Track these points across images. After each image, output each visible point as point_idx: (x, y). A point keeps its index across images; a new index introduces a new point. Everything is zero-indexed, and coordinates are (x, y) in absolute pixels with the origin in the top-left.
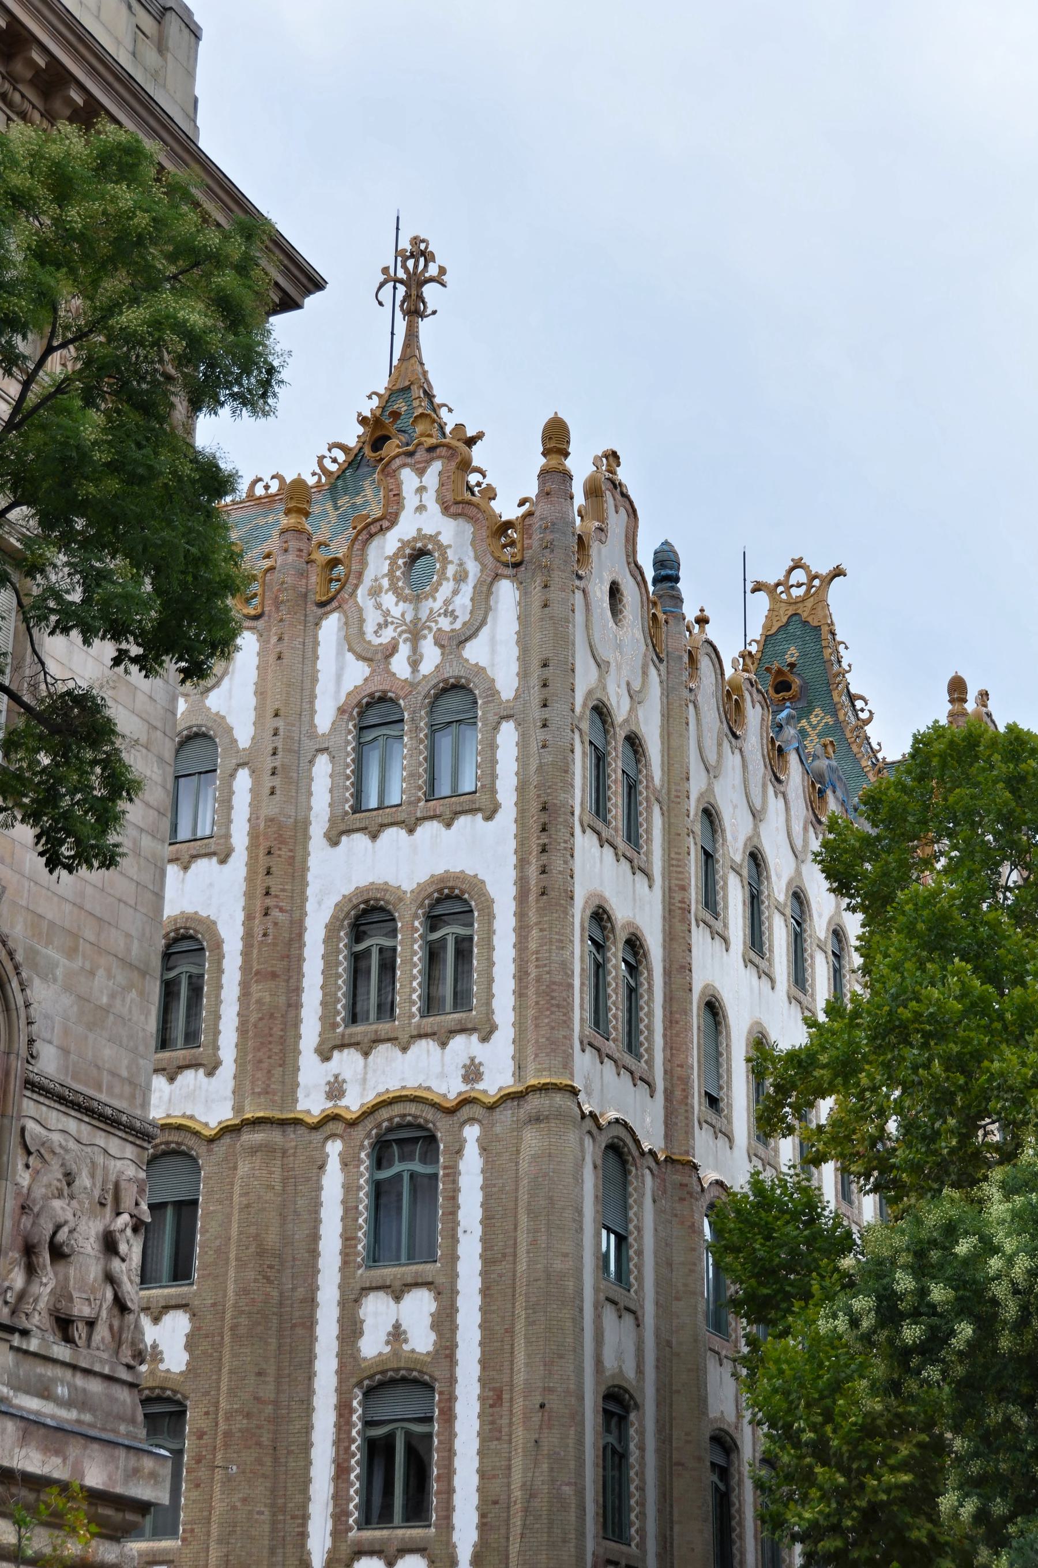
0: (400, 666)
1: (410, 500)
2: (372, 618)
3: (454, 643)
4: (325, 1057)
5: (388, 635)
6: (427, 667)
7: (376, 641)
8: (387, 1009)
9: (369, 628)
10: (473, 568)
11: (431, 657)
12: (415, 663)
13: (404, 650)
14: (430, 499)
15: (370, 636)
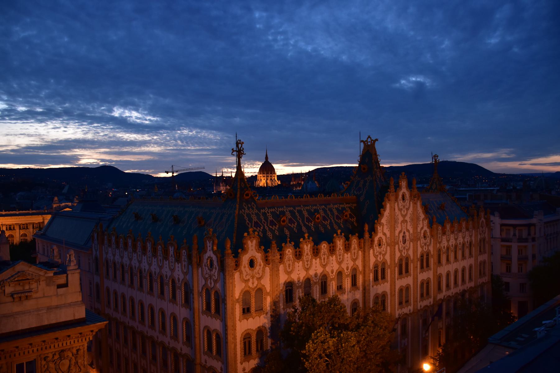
0: (250, 284)
1: (250, 249)
2: (245, 274)
3: (259, 279)
4: (242, 364)
5: (248, 277)
6: (255, 285)
7: (246, 279)
8: (250, 352)
9: (244, 276)
10: (262, 264)
11: (256, 283)
12: (253, 284)
13: (251, 280)
14: (254, 248)
15: (244, 277)
